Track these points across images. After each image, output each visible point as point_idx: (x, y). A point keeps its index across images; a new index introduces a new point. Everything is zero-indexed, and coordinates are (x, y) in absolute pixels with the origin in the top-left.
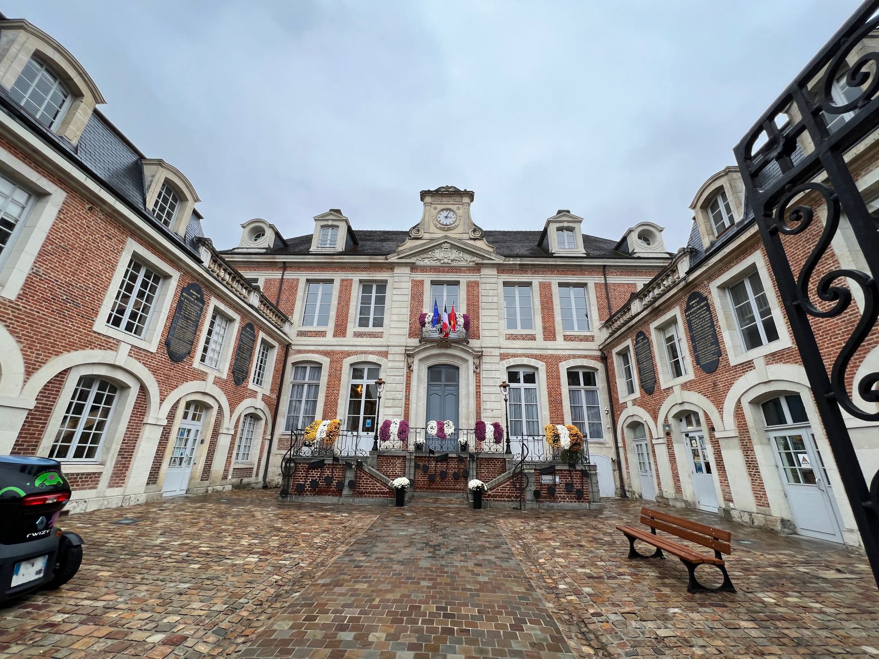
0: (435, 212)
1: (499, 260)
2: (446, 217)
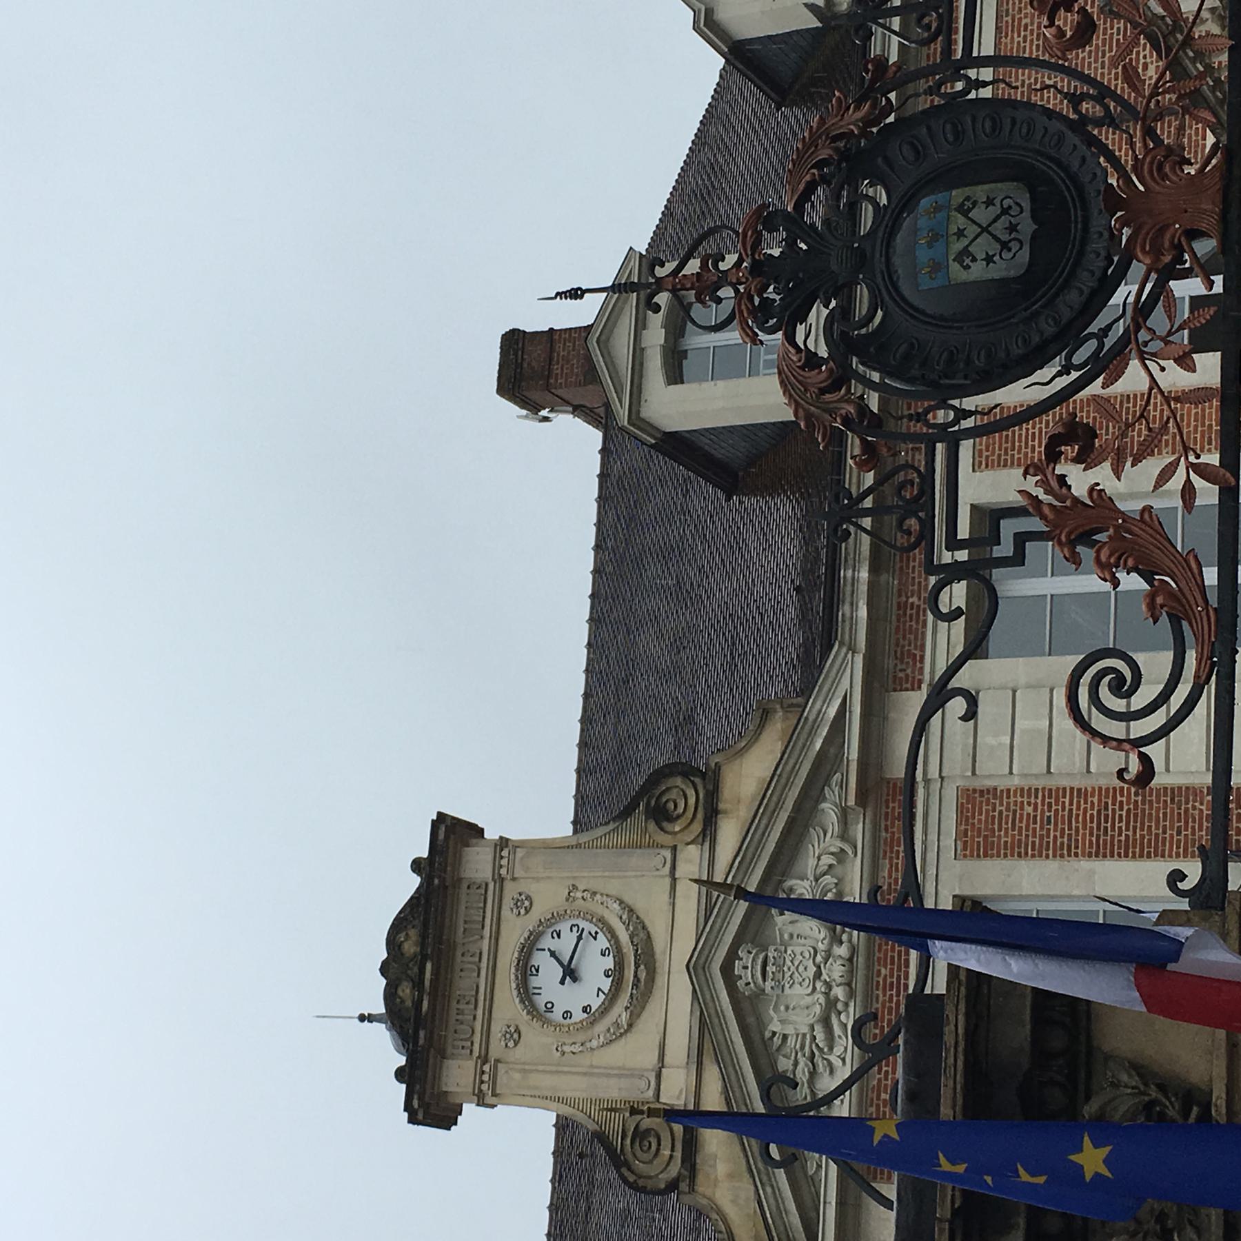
0: (536, 1039)
1: (846, 677)
2: (570, 973)
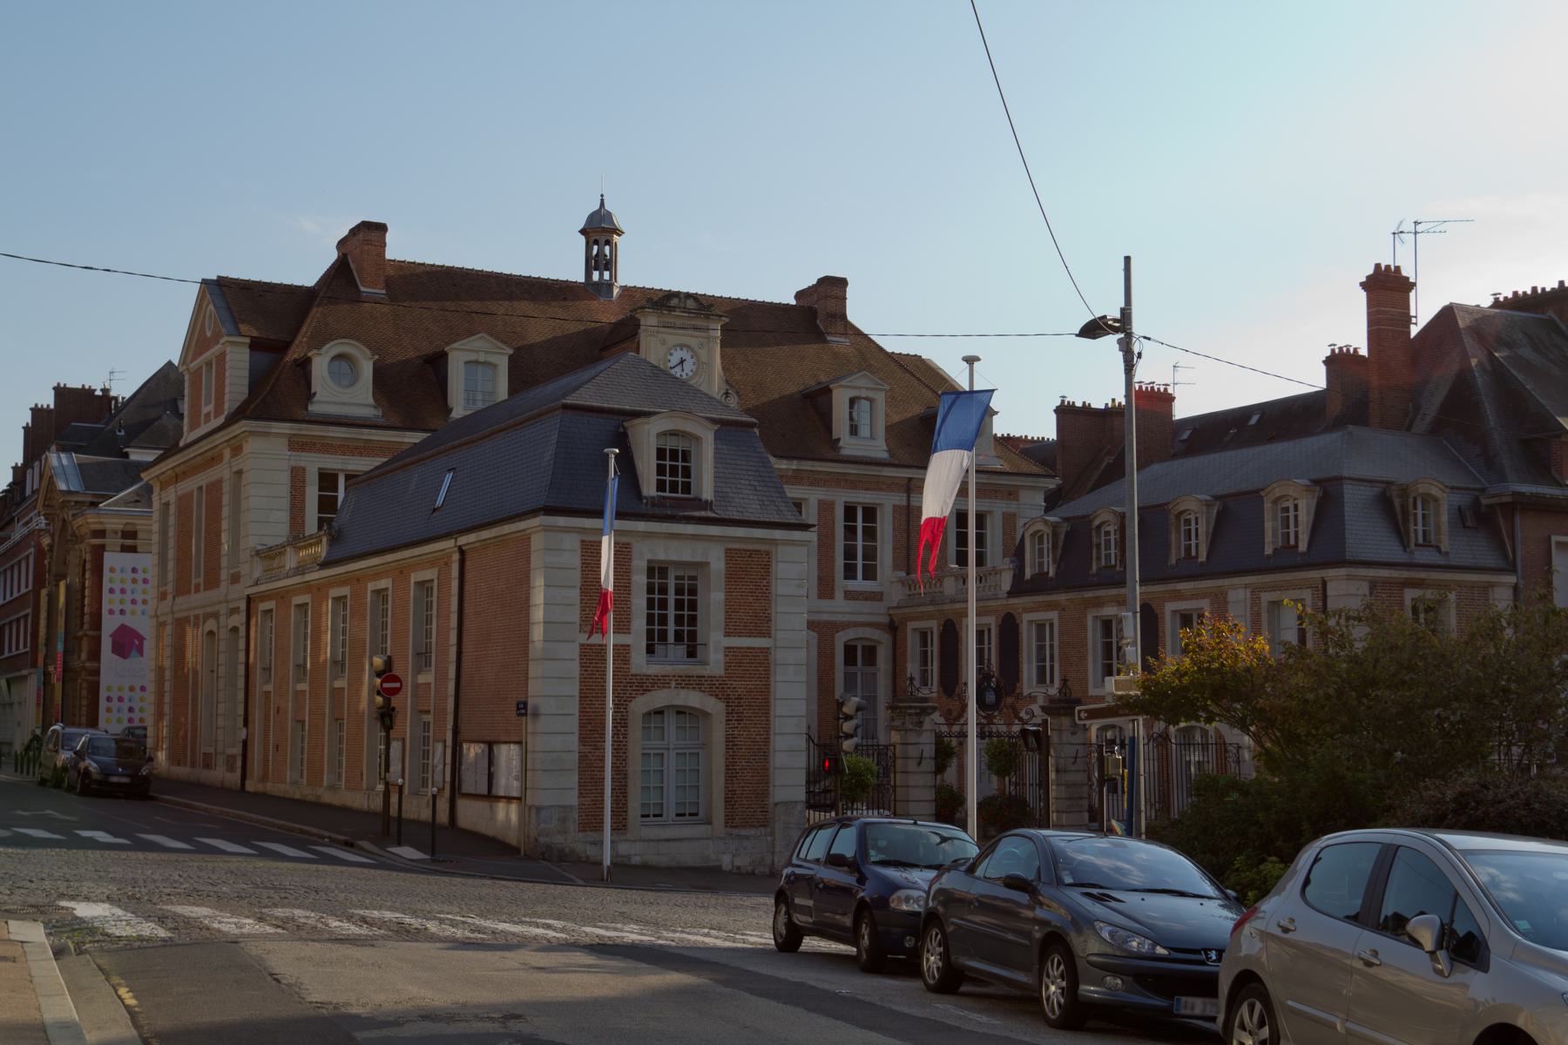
2: (682, 361)
